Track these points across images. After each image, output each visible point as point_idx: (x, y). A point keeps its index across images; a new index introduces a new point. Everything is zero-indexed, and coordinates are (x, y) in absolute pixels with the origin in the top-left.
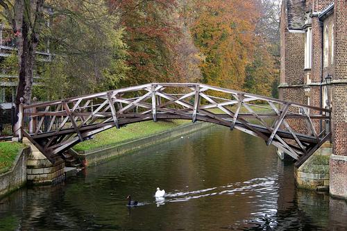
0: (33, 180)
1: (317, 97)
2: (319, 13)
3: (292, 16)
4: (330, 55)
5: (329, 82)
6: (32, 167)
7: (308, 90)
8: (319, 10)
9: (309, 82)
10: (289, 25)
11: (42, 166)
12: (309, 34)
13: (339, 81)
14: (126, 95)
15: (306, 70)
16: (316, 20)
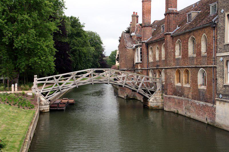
0: (43, 111)
1: (145, 73)
2: (146, 41)
3: (127, 42)
4: (154, 58)
5: (157, 68)
6: (42, 105)
7: (139, 71)
8: (145, 40)
9: (139, 68)
10: (127, 46)
11: (45, 105)
12: (139, 49)
13: (169, 67)
14: (78, 74)
15: (138, 63)
16: (144, 44)
